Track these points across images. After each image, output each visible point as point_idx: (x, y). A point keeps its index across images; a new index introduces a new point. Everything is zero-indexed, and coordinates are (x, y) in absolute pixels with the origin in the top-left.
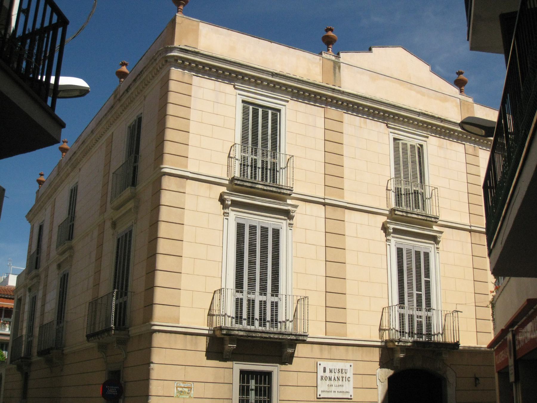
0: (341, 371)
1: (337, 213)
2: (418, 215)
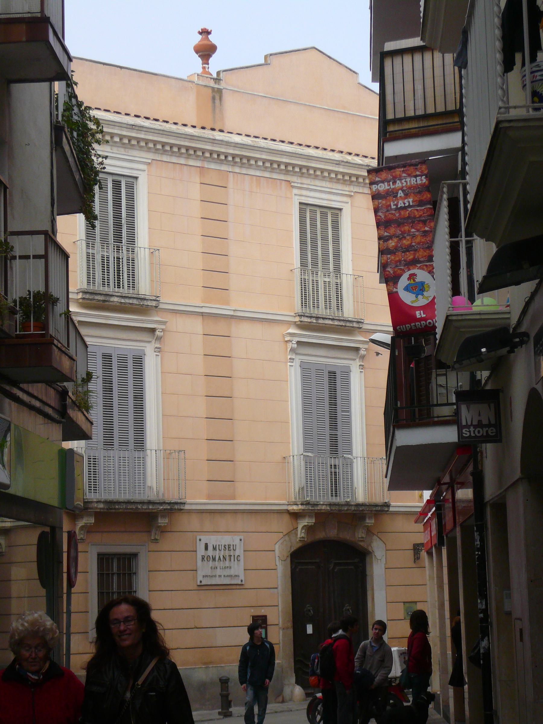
0: (228, 547)
1: (220, 328)
2: (333, 320)
